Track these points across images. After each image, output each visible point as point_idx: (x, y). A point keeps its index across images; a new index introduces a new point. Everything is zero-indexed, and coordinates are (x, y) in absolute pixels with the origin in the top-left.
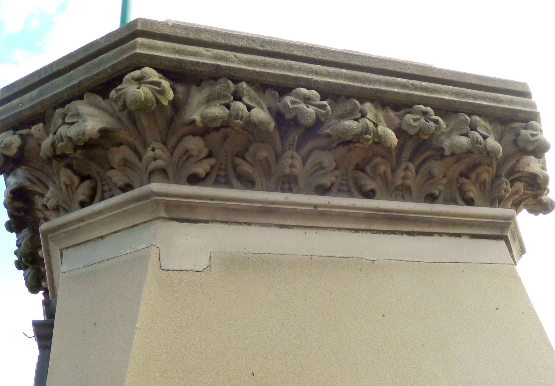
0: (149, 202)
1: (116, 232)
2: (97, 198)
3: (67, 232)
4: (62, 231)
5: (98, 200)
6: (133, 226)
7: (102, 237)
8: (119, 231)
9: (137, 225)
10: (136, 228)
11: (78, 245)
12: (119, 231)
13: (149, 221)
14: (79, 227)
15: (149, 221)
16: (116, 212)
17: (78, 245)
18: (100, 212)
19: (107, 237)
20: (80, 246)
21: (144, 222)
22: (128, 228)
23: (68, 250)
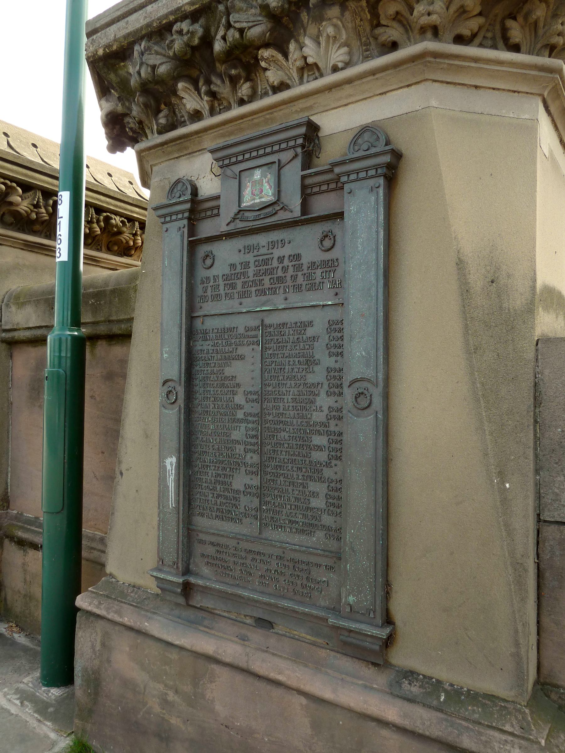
0: (550, 77)
1: (494, 89)
2: (477, 40)
3: (452, 65)
4: (447, 61)
5: (478, 44)
6: (515, 92)
7: (476, 87)
8: (498, 89)
9: (519, 92)
10: (516, 94)
11: (448, 83)
12: (498, 89)
13: (531, 94)
14: (469, 66)
15: (531, 94)
16: (515, 70)
17: (448, 83)
18: (500, 63)
19: (482, 90)
20: (449, 85)
21: (527, 93)
22: (509, 91)
23: (434, 83)
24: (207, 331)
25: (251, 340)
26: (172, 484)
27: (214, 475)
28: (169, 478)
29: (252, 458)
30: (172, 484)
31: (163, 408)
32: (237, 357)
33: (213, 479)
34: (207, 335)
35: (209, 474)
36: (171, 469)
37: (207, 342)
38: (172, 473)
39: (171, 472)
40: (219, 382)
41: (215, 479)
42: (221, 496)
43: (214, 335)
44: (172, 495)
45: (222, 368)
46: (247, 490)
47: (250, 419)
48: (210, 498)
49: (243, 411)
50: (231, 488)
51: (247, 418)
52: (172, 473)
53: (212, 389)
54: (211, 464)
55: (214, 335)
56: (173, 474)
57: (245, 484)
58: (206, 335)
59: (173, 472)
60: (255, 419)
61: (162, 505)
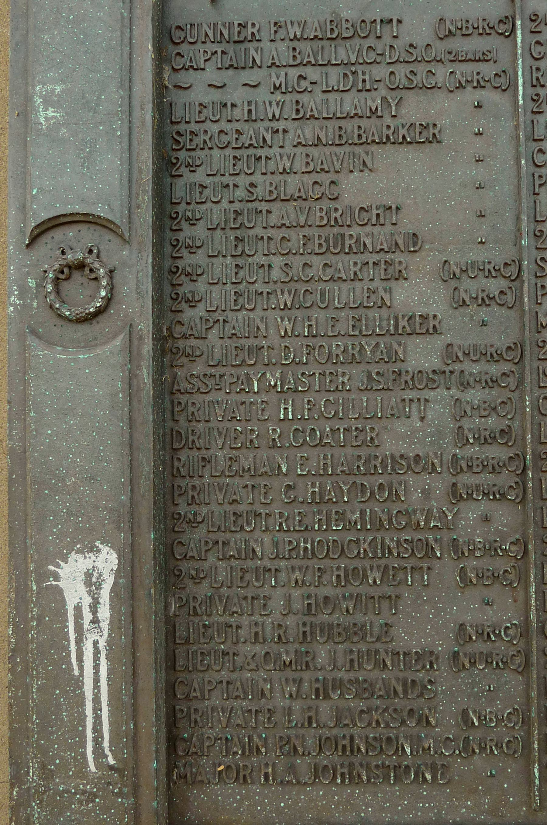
24: (250, 30)
25: (468, 68)
26: (96, 667)
27: (297, 606)
28: (79, 641)
29: (486, 519)
30: (96, 667)
31: (32, 341)
32: (402, 132)
33: (290, 621)
34: (251, 46)
35: (271, 604)
36: (87, 600)
37: (247, 72)
38: (95, 621)
39: (87, 616)
40: (315, 232)
41: (306, 619)
42: (338, 684)
43: (283, 47)
44: (97, 718)
45: (332, 176)
46: (469, 648)
47: (475, 369)
48: (281, 702)
49: (439, 342)
50: (390, 646)
51: (457, 367)
52: (95, 621)
53: (278, 261)
54: (283, 564)
55: (283, 47)
56: (105, 625)
57: (462, 626)
58: (243, 46)
59: (104, 613)
60: (495, 369)
61: (43, 767)
